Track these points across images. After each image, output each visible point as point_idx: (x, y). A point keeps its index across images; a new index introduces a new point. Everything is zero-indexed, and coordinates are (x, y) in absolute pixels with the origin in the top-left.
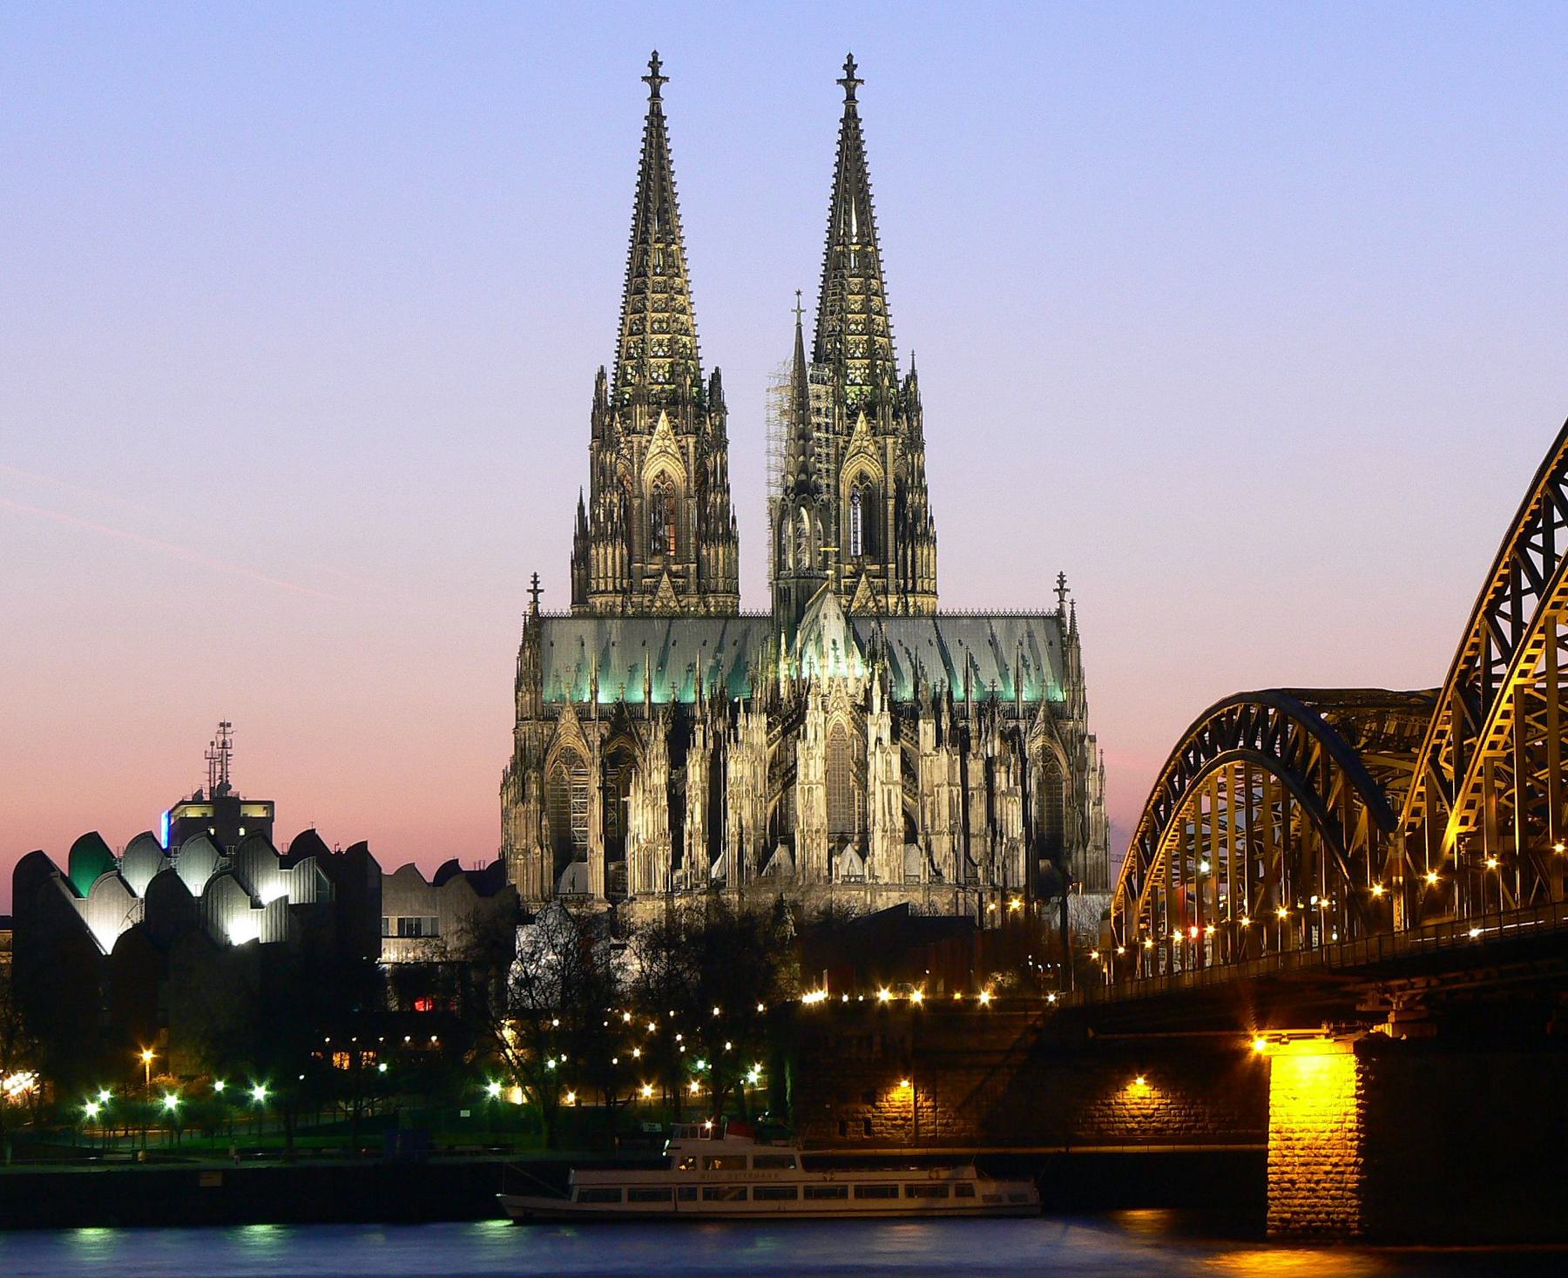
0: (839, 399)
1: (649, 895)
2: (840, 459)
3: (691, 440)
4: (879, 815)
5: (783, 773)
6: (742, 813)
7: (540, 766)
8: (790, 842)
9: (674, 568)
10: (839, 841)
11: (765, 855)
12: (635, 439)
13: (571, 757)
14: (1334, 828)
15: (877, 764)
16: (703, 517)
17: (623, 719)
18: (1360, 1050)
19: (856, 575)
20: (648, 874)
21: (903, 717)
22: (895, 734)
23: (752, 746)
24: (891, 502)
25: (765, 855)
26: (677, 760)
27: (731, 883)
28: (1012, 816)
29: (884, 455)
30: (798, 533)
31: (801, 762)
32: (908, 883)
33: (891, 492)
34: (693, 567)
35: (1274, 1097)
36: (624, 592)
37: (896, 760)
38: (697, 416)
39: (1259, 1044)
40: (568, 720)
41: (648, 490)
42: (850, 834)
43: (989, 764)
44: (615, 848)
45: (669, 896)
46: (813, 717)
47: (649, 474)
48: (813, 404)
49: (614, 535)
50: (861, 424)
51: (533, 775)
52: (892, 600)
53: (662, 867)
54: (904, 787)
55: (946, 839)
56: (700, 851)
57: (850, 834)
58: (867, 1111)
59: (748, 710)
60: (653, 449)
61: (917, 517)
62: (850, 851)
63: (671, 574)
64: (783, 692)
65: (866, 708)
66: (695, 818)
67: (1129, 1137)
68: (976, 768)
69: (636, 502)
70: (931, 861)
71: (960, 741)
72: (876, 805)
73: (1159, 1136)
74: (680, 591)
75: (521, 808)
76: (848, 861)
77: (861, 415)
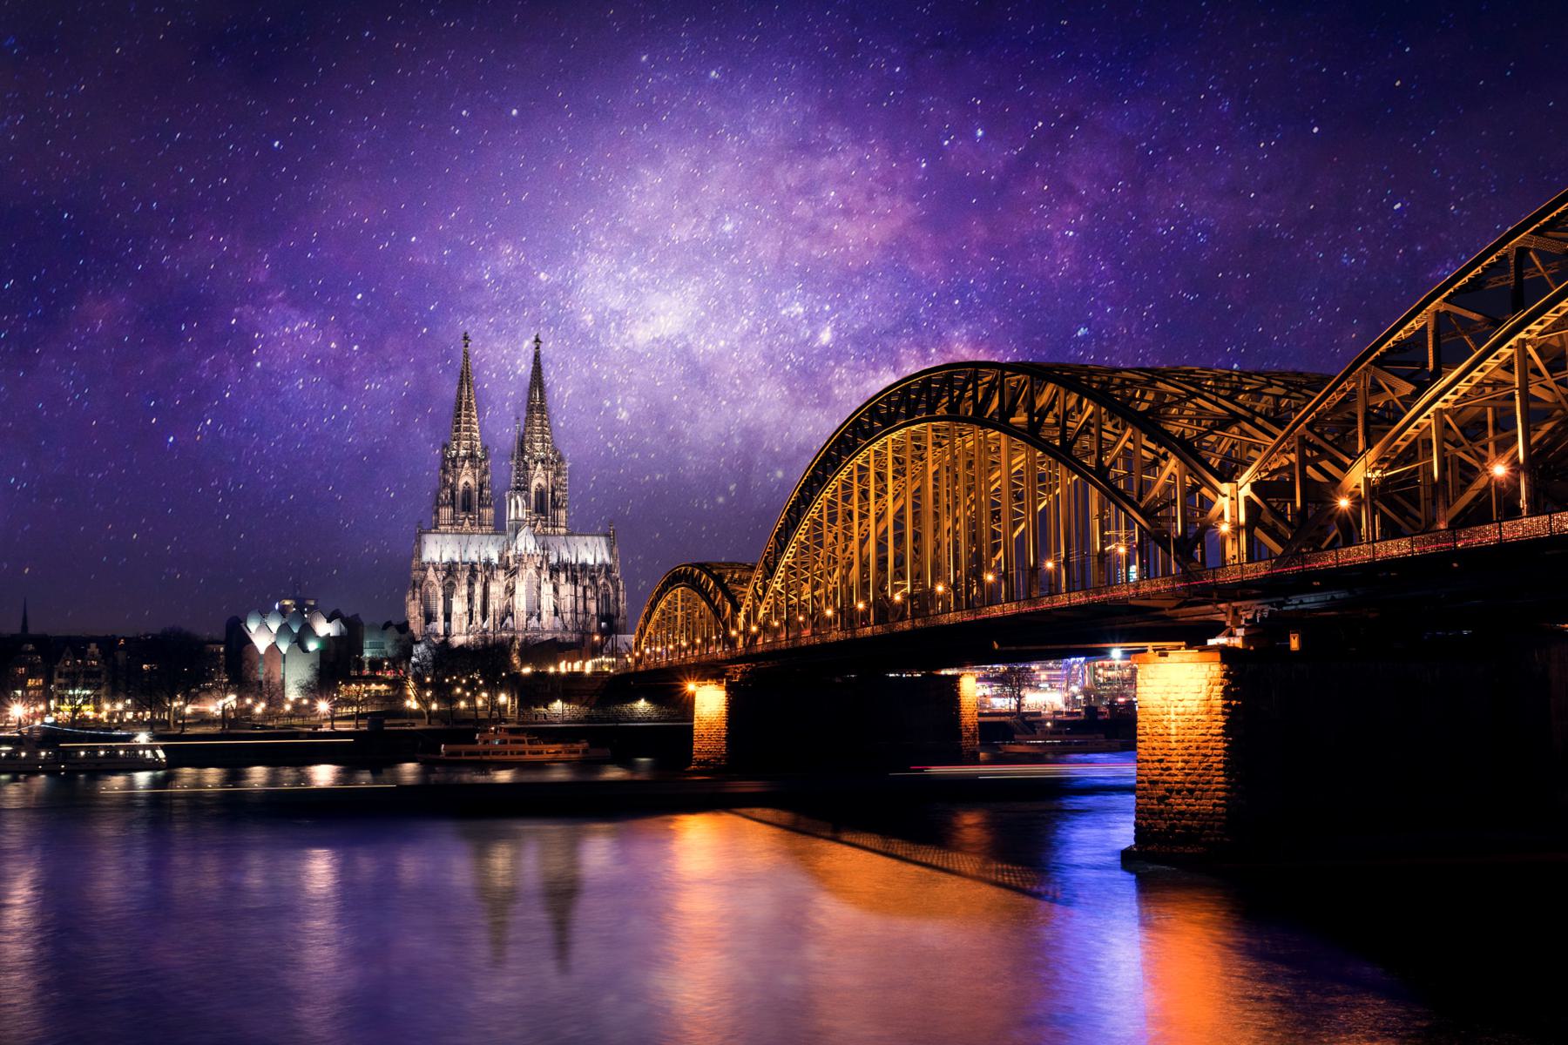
5: (510, 591)
6: (496, 604)
8: (512, 615)
10: (531, 615)
11: (503, 620)
13: (433, 584)
14: (718, 612)
16: (480, 498)
18: (728, 689)
25: (503, 620)
26: (471, 584)
28: (592, 606)
32: (555, 630)
39: (691, 687)
42: (535, 612)
43: (585, 588)
44: (448, 618)
47: (461, 483)
50: (539, 466)
53: (465, 624)
56: (479, 618)
57: (535, 612)
62: (534, 618)
65: (540, 568)
67: (640, 720)
68: (580, 589)
73: (649, 720)
76: (534, 622)
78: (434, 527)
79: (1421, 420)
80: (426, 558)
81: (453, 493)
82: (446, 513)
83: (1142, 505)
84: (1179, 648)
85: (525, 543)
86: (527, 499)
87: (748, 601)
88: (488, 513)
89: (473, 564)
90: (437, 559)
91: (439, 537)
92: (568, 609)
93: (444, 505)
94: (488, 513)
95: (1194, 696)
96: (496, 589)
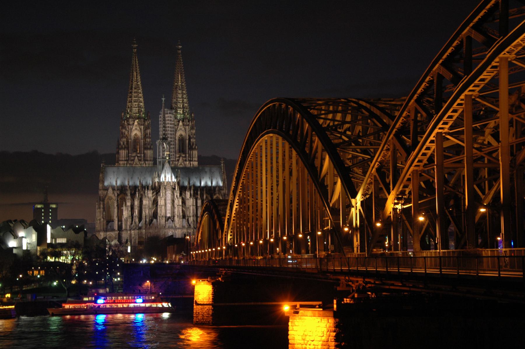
0: (176, 118)
1: (126, 230)
2: (176, 131)
3: (142, 127)
4: (176, 213)
5: (155, 202)
6: (146, 212)
7: (103, 201)
8: (156, 218)
9: (139, 155)
11: (152, 220)
12: (130, 126)
13: (110, 198)
15: (176, 202)
16: (145, 144)
17: (122, 190)
18: (213, 284)
19: (179, 157)
20: (126, 225)
21: (183, 189)
22: (181, 194)
23: (148, 197)
24: (187, 141)
27: (144, 227)
29: (186, 130)
30: (164, 148)
31: (159, 201)
32: (183, 227)
33: (187, 139)
34: (143, 155)
35: (196, 294)
36: (127, 160)
37: (180, 200)
38: (144, 121)
39: (194, 282)
40: (110, 190)
41: (133, 138)
44: (120, 220)
45: (130, 230)
47: (133, 134)
48: (167, 119)
49: (125, 147)
50: (181, 123)
51: (102, 203)
52: (187, 163)
53: (129, 223)
54: (182, 206)
55: (192, 218)
56: (137, 220)
58: (140, 288)
59: (148, 189)
60: (134, 128)
61: (193, 144)
63: (138, 157)
64: (157, 185)
65: (174, 189)
66: (136, 213)
68: (199, 202)
69: (130, 141)
70: (188, 223)
71: (194, 195)
74: (140, 160)
75: (99, 210)
76: (169, 223)
77: (181, 122)
79: (407, 176)
81: (128, 142)
82: (123, 153)
83: (331, 205)
84: (313, 307)
86: (169, 144)
87: (225, 230)
88: (149, 153)
90: (114, 184)
91: (115, 169)
92: (191, 214)
93: (122, 148)
95: (319, 338)
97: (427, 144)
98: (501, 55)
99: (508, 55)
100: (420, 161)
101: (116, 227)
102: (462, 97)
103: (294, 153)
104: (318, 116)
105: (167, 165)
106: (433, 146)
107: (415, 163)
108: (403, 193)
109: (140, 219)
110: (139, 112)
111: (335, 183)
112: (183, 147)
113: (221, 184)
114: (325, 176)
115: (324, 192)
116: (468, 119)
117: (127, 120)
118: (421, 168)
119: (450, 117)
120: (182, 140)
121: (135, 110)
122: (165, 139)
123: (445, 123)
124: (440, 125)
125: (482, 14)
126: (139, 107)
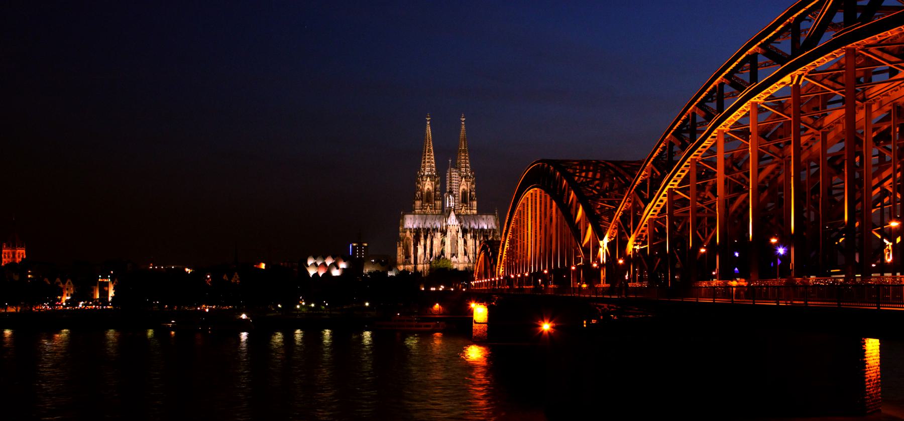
0: (460, 175)
5: (443, 243)
6: (436, 250)
13: (408, 239)
17: (417, 233)
21: (465, 232)
25: (439, 257)
32: (464, 262)
40: (408, 232)
46: (449, 233)
47: (426, 188)
68: (478, 242)
71: (474, 237)
72: (459, 249)
76: (454, 259)
78: (411, 210)
80: (406, 226)
82: (418, 203)
85: (452, 220)
86: (454, 196)
88: (439, 203)
89: (429, 229)
91: (412, 216)
94: (439, 203)
96: (437, 242)
97: (661, 197)
98: (719, 128)
99: (723, 128)
100: (655, 211)
101: (412, 261)
102: (689, 160)
103: (554, 203)
104: (574, 175)
105: (452, 214)
106: (665, 199)
107: (651, 212)
108: (641, 236)
109: (431, 255)
110: (431, 171)
111: (587, 228)
112: (465, 199)
113: (495, 227)
114: (579, 221)
115: (578, 235)
116: (693, 177)
117: (422, 177)
118: (656, 217)
119: (679, 176)
120: (464, 193)
121: (428, 169)
122: (451, 192)
123: (675, 181)
124: (671, 183)
125: (704, 95)
126: (431, 166)
